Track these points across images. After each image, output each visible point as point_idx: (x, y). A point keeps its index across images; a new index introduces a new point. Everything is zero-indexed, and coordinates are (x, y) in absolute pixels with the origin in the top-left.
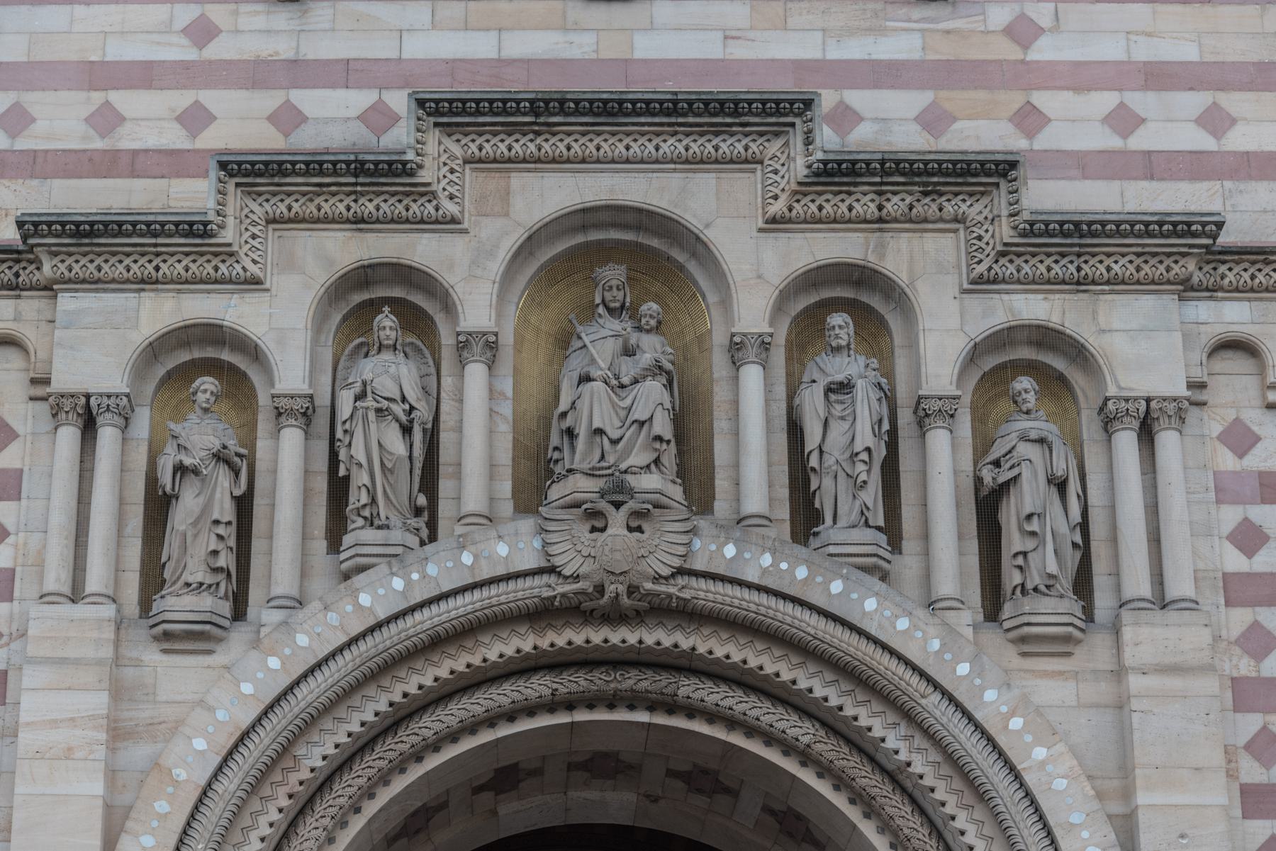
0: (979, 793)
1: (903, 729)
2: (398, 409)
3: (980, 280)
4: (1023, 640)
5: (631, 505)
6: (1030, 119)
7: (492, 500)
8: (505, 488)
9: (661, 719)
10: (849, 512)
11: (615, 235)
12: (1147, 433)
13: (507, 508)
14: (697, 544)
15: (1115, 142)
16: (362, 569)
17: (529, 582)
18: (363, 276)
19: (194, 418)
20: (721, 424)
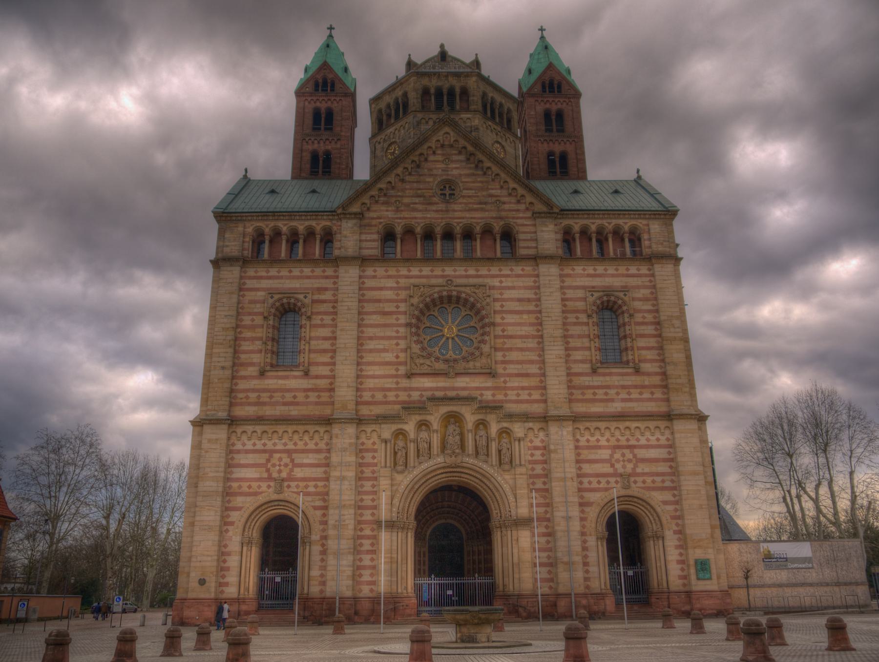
0: (498, 490)
12: (519, 441)
13: (439, 453)
15: (517, 398)
20: (466, 441)
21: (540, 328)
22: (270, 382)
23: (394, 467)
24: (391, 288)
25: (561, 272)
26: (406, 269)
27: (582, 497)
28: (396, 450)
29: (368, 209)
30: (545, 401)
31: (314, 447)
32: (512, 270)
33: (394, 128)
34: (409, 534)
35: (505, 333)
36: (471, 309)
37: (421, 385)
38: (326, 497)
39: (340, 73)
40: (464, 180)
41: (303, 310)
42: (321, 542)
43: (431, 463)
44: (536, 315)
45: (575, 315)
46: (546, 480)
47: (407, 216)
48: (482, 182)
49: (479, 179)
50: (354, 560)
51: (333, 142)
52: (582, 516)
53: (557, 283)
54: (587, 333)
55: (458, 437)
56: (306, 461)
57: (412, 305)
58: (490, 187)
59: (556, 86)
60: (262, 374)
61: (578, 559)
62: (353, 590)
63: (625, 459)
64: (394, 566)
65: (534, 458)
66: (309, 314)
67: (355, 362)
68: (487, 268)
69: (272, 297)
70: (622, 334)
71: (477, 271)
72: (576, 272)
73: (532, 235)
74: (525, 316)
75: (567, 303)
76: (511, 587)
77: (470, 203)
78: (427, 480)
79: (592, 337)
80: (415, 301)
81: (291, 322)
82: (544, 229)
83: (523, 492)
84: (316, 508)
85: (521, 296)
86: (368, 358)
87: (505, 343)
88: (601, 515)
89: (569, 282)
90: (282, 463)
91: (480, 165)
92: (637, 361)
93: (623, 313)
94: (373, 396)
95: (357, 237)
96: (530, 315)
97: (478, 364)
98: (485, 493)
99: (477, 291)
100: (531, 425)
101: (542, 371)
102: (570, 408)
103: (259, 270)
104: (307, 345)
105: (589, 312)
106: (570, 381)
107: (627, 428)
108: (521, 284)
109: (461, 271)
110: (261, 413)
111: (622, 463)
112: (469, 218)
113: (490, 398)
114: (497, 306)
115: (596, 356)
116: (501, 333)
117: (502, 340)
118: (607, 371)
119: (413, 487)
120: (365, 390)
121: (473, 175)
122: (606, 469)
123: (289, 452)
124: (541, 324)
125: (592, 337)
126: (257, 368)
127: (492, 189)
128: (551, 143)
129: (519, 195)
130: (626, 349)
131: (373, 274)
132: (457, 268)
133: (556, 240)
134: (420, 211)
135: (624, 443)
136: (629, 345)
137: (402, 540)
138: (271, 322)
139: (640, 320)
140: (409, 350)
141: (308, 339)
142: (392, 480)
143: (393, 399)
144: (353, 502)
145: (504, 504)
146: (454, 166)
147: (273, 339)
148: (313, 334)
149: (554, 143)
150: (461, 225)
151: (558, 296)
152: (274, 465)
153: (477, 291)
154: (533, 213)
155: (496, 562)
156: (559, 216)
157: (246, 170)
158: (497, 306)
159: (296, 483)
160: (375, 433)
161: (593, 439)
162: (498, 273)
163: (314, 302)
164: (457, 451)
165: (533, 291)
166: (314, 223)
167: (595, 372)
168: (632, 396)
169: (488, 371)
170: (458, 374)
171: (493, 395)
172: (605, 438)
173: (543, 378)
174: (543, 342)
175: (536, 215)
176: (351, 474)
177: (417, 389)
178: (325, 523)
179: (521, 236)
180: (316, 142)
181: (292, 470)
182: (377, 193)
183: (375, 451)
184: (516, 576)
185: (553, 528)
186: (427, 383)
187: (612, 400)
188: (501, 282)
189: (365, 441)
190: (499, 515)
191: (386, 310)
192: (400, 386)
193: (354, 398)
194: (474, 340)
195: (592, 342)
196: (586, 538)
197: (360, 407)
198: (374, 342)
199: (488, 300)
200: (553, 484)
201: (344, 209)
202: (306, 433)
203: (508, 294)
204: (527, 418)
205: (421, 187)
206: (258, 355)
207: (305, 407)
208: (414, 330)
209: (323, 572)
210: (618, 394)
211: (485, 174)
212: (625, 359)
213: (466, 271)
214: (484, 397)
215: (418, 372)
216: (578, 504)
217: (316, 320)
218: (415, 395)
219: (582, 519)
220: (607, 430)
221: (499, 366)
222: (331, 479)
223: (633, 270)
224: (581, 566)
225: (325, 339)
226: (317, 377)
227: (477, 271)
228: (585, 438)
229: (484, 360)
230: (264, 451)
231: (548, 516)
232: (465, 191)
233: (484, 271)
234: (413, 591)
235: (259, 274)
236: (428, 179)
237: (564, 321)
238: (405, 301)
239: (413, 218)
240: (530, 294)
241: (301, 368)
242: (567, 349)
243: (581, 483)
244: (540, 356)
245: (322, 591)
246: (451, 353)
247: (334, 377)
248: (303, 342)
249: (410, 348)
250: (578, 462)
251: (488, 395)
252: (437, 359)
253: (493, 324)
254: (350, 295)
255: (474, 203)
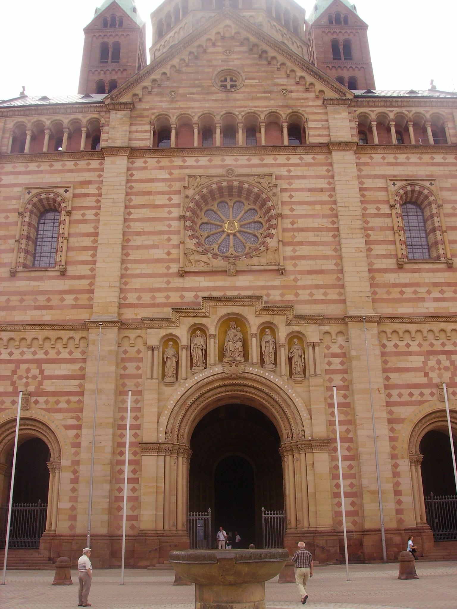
0: (289, 406)
1: (277, 396)
2: (200, 347)
3: (288, 324)
4: (295, 381)
5: (236, 362)
6: (297, 295)
7: (215, 361)
8: (217, 358)
9: (242, 393)
10: (269, 362)
11: (233, 316)
12: (314, 347)
13: (217, 362)
14: (246, 368)
15: (310, 298)
16: (196, 373)
17: (221, 374)
18: (195, 325)
19: (169, 349)
21: (335, 220)
22: (21, 284)
23: (163, 379)
24: (163, 180)
25: (358, 161)
26: (181, 159)
27: (391, 413)
28: (165, 359)
29: (140, 100)
30: (344, 301)
31: (67, 356)
32: (301, 159)
33: (174, 32)
34: (180, 459)
35: (295, 226)
36: (255, 203)
37: (196, 285)
38: (80, 415)
39: (129, 13)
40: (245, 70)
41: (63, 205)
42: (72, 469)
43: (207, 373)
44: (330, 206)
45: (375, 206)
46: (347, 393)
47: (182, 106)
48: (266, 72)
49: (263, 69)
50: (111, 491)
51: (120, 72)
52: (392, 435)
53: (353, 170)
54: (390, 225)
55: (239, 344)
56: (57, 372)
57: (187, 197)
58: (274, 76)
59: (342, 20)
60: (13, 274)
61: (389, 487)
62: (109, 525)
63: (442, 366)
64: (161, 497)
65: (332, 367)
66: (69, 208)
67: (120, 260)
68: (273, 156)
69: (29, 193)
70: (429, 227)
71: (262, 160)
72: (374, 160)
73: (324, 123)
74: (318, 207)
75: (365, 193)
76: (306, 524)
77: (253, 92)
78: (200, 397)
79: (396, 229)
80: (190, 192)
81: (50, 221)
82: (336, 116)
83: (319, 406)
84: (68, 427)
85: (313, 186)
86: (134, 255)
87: (295, 237)
88: (414, 434)
89: (366, 171)
90: (30, 375)
91: (264, 55)
92: (449, 256)
93: (430, 204)
94: (139, 298)
95: (127, 128)
96: (324, 206)
97: (263, 260)
98: (273, 410)
99: (261, 181)
100: (327, 328)
101: (339, 268)
102: (374, 309)
103: (17, 165)
104: (65, 242)
105: (392, 202)
106: (373, 278)
107: (442, 330)
108: (312, 173)
109: (243, 160)
110: (9, 319)
111: (437, 371)
112: (251, 107)
113: (278, 298)
114: (285, 196)
115: (402, 250)
116: (290, 226)
117: (292, 233)
118: (416, 266)
119: (184, 402)
120: (130, 291)
121: (257, 64)
122: (419, 378)
123: (39, 362)
124: (336, 216)
125: (396, 229)
126: (7, 269)
127: (278, 78)
128: (339, 70)
129: (308, 84)
130: (436, 243)
131: (144, 165)
132: (240, 158)
133: (351, 128)
134: (198, 101)
135: (439, 348)
136: (439, 238)
137: (170, 466)
138: (27, 219)
139: (451, 211)
140: (182, 245)
141: (66, 235)
142: (159, 393)
143: (164, 301)
144: (111, 420)
145: (296, 422)
146: (235, 57)
147: (28, 238)
148: (72, 231)
149: (342, 70)
150: (243, 114)
151: (356, 185)
152: (21, 377)
153: (261, 181)
154: (324, 100)
155: (287, 492)
156: (353, 104)
157: (24, 88)
158: (285, 196)
159: (45, 398)
160: (140, 339)
161: (402, 344)
162: (286, 162)
163: (75, 196)
164: (239, 358)
165: (326, 181)
166: (80, 116)
167: (402, 268)
168: (445, 295)
169: (275, 267)
170: (239, 272)
171: (282, 295)
172: (416, 343)
173: (340, 275)
174: (339, 235)
175: (327, 102)
176: (111, 386)
177: (191, 289)
178: (78, 445)
179: (311, 125)
180: (102, 72)
181: (41, 383)
182: (150, 84)
183: (140, 360)
184: (312, 509)
185: (357, 449)
186: (203, 282)
187: (423, 300)
188: (289, 171)
189: (129, 349)
190: (290, 435)
191: (157, 202)
192: (171, 285)
193: (116, 300)
194: (259, 236)
195: (397, 235)
196: (397, 461)
197: (123, 310)
198: (143, 237)
199: (274, 190)
200: (356, 397)
201: (112, 99)
202: (59, 341)
203: (297, 184)
204: (323, 320)
205: (199, 77)
206: (10, 255)
207: (59, 312)
208: (188, 223)
209: (75, 504)
210: (429, 292)
211: (269, 63)
212: (435, 254)
213: (249, 160)
214: (271, 298)
215: (193, 269)
216: (386, 421)
217: (77, 215)
218: (189, 296)
219: (391, 439)
220: (419, 333)
221: (288, 262)
222: (85, 392)
223: (438, 158)
224: (393, 495)
225: (88, 235)
226: (74, 277)
227: (262, 160)
228: (393, 343)
229: (270, 256)
230: (10, 362)
231: (350, 435)
232: (246, 81)
233: (269, 160)
234: (185, 529)
235: (17, 170)
236: (206, 70)
237: (364, 212)
238: (179, 192)
239: (189, 108)
240: (322, 184)
241: (58, 268)
242: (367, 243)
243: (389, 395)
244: (336, 250)
245: (72, 527)
246: (231, 250)
247: (94, 277)
248: (61, 240)
249: (184, 243)
250: (385, 370)
251: (276, 296)
252: (215, 256)
253: (280, 216)
254: (116, 187)
255: (258, 92)
